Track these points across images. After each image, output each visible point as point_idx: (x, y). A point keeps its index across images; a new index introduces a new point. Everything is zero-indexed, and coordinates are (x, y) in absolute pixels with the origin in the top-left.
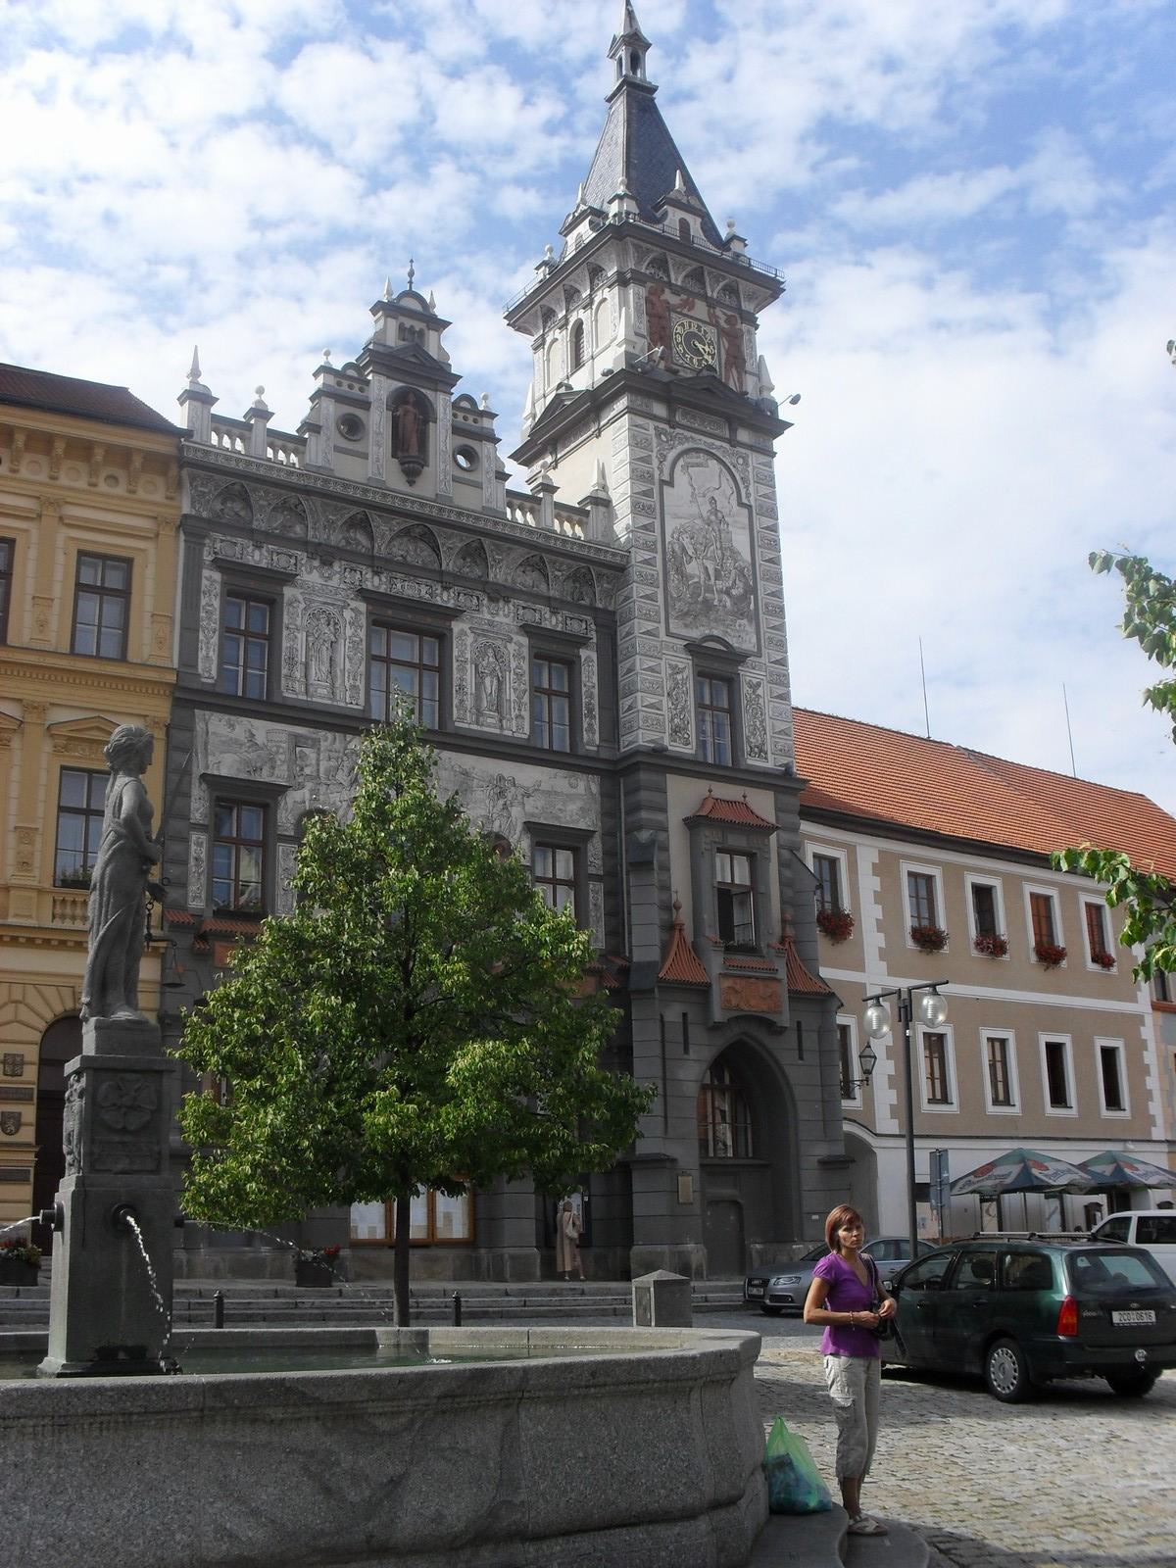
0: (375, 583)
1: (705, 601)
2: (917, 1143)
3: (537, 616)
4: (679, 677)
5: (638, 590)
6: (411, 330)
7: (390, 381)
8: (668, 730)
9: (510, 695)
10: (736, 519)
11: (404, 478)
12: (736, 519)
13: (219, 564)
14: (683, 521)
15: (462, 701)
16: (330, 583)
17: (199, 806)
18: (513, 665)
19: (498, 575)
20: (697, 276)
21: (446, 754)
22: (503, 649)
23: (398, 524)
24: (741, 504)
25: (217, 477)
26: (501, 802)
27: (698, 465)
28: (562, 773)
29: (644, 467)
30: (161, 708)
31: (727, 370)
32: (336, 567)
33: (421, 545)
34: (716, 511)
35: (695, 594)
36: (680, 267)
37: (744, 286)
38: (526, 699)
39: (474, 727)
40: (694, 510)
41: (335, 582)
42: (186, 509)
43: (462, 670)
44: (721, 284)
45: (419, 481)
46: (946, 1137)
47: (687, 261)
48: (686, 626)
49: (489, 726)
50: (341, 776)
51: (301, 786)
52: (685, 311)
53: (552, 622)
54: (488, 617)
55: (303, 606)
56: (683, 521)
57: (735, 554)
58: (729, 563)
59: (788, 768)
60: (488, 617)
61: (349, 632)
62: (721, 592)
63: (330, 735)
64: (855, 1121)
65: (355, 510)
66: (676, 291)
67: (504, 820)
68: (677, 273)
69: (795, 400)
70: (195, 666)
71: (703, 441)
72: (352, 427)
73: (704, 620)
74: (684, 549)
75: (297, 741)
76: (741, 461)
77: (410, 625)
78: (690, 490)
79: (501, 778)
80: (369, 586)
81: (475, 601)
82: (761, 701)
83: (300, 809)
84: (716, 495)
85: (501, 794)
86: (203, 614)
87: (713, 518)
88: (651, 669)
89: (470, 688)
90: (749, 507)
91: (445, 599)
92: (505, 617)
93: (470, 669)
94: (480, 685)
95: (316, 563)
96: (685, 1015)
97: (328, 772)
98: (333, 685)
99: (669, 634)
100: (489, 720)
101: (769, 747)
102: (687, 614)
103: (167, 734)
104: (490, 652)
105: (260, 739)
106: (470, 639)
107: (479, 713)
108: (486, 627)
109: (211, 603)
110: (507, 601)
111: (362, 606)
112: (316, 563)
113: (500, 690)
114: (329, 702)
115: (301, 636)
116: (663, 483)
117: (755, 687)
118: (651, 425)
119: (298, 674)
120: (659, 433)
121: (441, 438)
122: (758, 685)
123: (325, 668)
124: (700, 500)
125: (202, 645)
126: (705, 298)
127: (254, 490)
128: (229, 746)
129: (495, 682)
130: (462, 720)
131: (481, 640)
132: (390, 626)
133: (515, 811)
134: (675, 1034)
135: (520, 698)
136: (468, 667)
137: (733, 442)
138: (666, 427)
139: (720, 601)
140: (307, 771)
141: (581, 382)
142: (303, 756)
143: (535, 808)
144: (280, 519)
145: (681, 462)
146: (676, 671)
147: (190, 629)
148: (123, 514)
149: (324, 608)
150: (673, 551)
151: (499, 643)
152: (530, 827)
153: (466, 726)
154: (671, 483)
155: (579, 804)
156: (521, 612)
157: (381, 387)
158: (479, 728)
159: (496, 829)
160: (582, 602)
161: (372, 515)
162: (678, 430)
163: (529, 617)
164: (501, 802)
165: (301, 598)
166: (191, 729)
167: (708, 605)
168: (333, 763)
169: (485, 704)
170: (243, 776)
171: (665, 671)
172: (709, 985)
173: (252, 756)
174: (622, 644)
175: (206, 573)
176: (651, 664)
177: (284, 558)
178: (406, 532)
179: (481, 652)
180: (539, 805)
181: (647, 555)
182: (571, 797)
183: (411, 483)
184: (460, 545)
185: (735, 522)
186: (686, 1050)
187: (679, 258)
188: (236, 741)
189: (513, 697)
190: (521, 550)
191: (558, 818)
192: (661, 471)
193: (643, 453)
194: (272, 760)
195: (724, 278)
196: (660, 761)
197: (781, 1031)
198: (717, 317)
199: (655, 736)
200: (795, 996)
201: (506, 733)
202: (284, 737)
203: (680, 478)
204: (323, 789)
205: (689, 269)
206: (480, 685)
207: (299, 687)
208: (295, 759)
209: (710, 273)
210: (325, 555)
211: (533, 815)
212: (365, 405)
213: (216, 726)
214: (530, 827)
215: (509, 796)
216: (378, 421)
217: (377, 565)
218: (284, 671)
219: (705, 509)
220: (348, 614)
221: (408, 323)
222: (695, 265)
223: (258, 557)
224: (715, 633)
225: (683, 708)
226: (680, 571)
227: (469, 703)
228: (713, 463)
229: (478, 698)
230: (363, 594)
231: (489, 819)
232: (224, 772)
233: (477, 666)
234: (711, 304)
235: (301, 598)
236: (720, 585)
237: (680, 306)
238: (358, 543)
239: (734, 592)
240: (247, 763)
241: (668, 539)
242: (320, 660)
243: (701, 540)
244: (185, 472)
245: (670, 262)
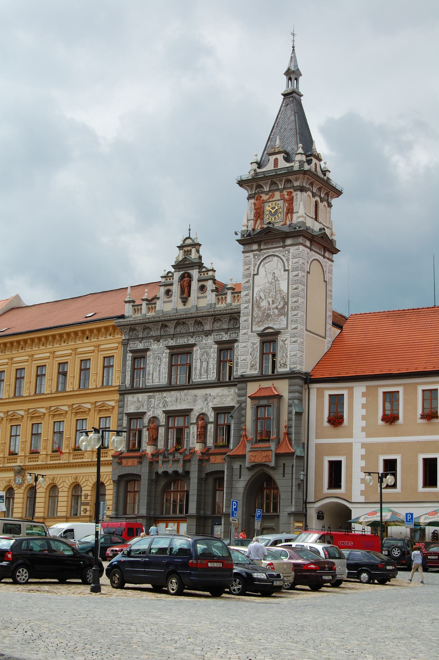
0: (172, 343)
1: (268, 314)
2: (384, 506)
3: (221, 336)
4: (255, 346)
5: (242, 319)
6: (188, 251)
7: (180, 272)
8: (249, 367)
9: (211, 366)
10: (283, 277)
11: (182, 304)
12: (283, 277)
13: (131, 351)
14: (261, 287)
15: (195, 373)
16: (160, 347)
18: (212, 356)
19: (207, 327)
20: (273, 183)
21: (190, 391)
22: (209, 351)
24: (285, 270)
26: (206, 402)
27: (269, 262)
28: (226, 388)
29: (248, 272)
30: (117, 397)
31: (286, 216)
32: (161, 341)
33: (185, 325)
36: (266, 184)
38: (216, 366)
39: (199, 380)
40: (266, 280)
41: (160, 346)
42: (124, 338)
43: (196, 362)
44: (283, 181)
45: (187, 304)
46: (431, 502)
47: (266, 181)
48: (259, 326)
49: (204, 379)
50: (161, 405)
51: (150, 410)
52: (271, 200)
53: (226, 337)
54: (205, 342)
55: (152, 356)
56: (261, 287)
57: (280, 291)
58: (278, 296)
60: (205, 342)
61: (164, 360)
62: (274, 308)
63: (158, 394)
64: (325, 498)
65: (161, 323)
66: (266, 193)
67: (206, 408)
68: (266, 187)
70: (125, 383)
71: (271, 252)
72: (168, 293)
73: (266, 321)
74: (261, 298)
75: (150, 397)
76: (287, 252)
78: (265, 273)
79: (206, 394)
80: (170, 344)
81: (201, 338)
82: (286, 346)
83: (150, 417)
85: (206, 400)
86: (127, 367)
87: (273, 281)
88: (245, 347)
89: (198, 368)
90: (288, 270)
91: (192, 341)
92: (210, 340)
93: (199, 361)
95: (156, 342)
96: (241, 466)
97: (157, 405)
98: (159, 378)
99: (252, 331)
100: (204, 376)
101: (288, 363)
102: (260, 322)
104: (205, 354)
105: (140, 400)
106: (199, 350)
107: (201, 374)
108: (204, 346)
110: (211, 335)
111: (168, 351)
112: (156, 342)
113: (207, 366)
114: (158, 383)
115: (151, 366)
116: (254, 275)
117: (284, 341)
118: (251, 254)
119: (150, 377)
120: (254, 255)
121: (195, 285)
122: (286, 340)
123: (157, 373)
124: (268, 276)
125: (127, 376)
126: (278, 190)
128: (133, 403)
129: (206, 363)
130: (195, 379)
131: (203, 350)
132: (178, 354)
134: (237, 472)
135: (214, 366)
136: (198, 361)
137: (284, 247)
138: (257, 252)
139: (273, 312)
140: (152, 406)
142: (151, 401)
143: (218, 403)
144: (147, 331)
145: (262, 263)
146: (254, 344)
147: (124, 372)
148: (111, 344)
149: (158, 355)
150: (257, 300)
151: (208, 350)
152: (214, 409)
153: (196, 380)
154: (257, 274)
155: (231, 397)
156: (215, 337)
157: (177, 275)
158: (200, 380)
159: (204, 412)
160: (237, 326)
161: (166, 323)
162: (262, 252)
163: (218, 338)
164: (206, 402)
165: (152, 354)
166: (124, 401)
167: (268, 316)
168: (159, 402)
169: (203, 371)
170: (135, 411)
171: (249, 345)
175: (128, 355)
176: (244, 345)
177: (147, 343)
178: (177, 324)
179: (202, 355)
180: (218, 400)
181: (246, 305)
182: (228, 396)
183: (184, 305)
184: (193, 322)
185: (282, 278)
186: (240, 478)
187: (263, 182)
188: (134, 402)
189: (212, 367)
190: (209, 318)
191: (224, 404)
192: (254, 270)
193: (247, 267)
194: (143, 405)
195: (283, 179)
196: (245, 380)
197: (273, 468)
198: (283, 195)
200: (278, 456)
201: (209, 379)
202: (146, 397)
203: (261, 269)
204: (156, 410)
205: (269, 183)
207: (150, 381)
208: (149, 403)
209: (277, 180)
210: (157, 339)
211: (216, 404)
213: (130, 398)
214: (214, 409)
215: (208, 400)
216: (176, 289)
217: (173, 336)
218: (147, 377)
219: (270, 277)
220: (164, 355)
221: (186, 249)
223: (140, 346)
224: (270, 325)
225: (256, 357)
226: (259, 307)
227: (198, 373)
228: (275, 259)
229: (201, 370)
230: (169, 347)
231: (202, 409)
232: (131, 411)
233: (201, 360)
234: (281, 191)
235: (152, 354)
236: (274, 306)
237: (269, 199)
238: (167, 331)
239: (279, 307)
240: (137, 407)
241: (255, 295)
242: (156, 371)
243: (268, 291)
245: (262, 184)
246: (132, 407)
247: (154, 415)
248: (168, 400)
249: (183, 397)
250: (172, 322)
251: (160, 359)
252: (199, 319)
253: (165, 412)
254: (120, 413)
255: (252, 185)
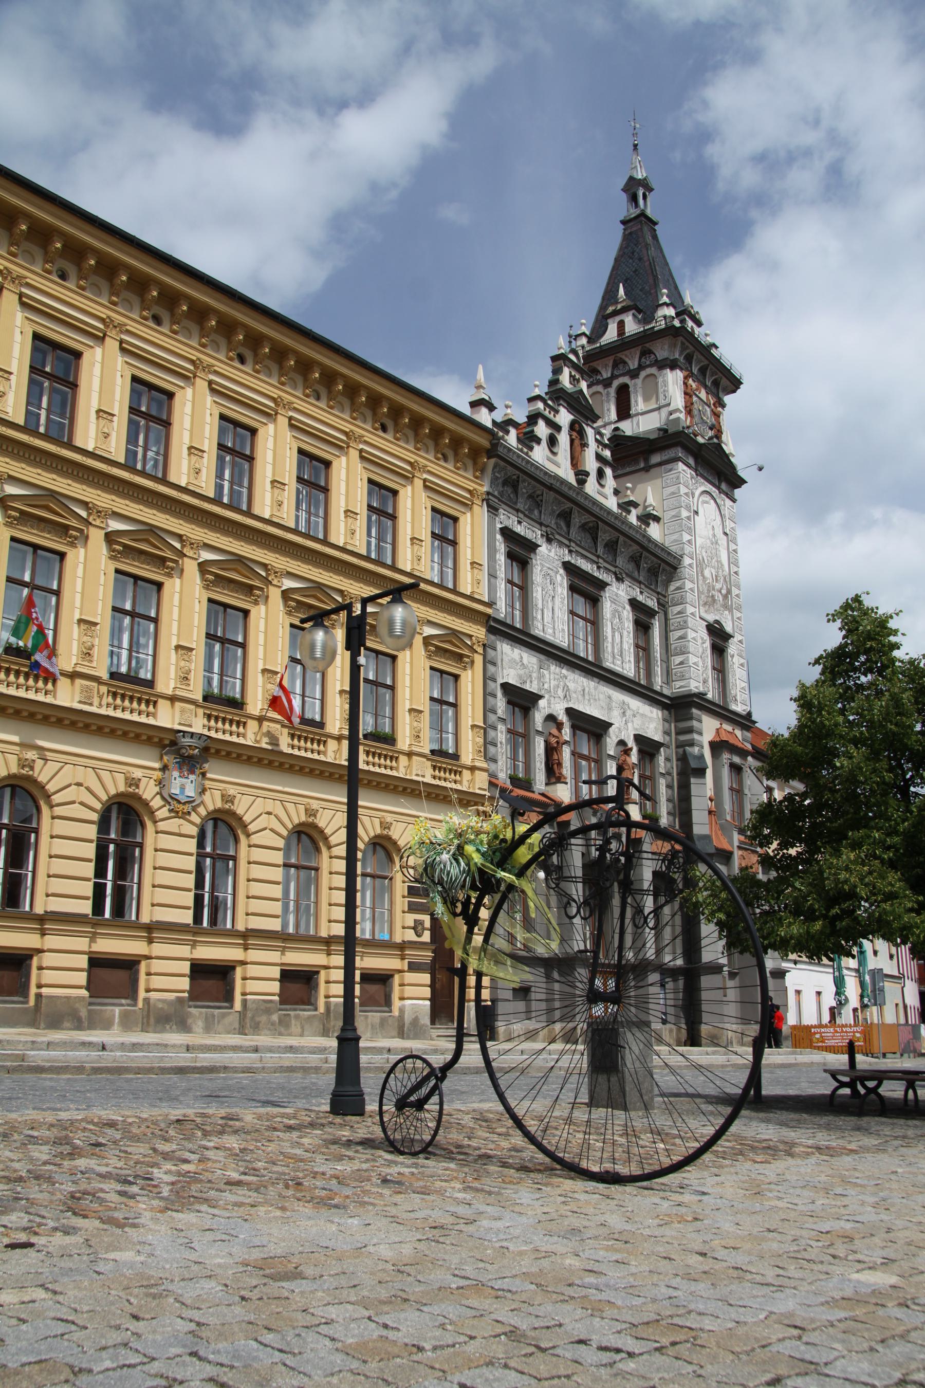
9: (625, 646)
17: (501, 704)
23: (586, 518)
25: (509, 468)
27: (707, 502)
33: (588, 535)
34: (714, 536)
35: (709, 591)
36: (699, 361)
37: (724, 382)
50: (560, 693)
59: (749, 714)
65: (569, 505)
69: (760, 469)
71: (709, 487)
77: (586, 590)
84: (714, 523)
89: (610, 639)
94: (613, 636)
103: (484, 650)
105: (525, 661)
107: (614, 657)
109: (501, 558)
115: (540, 589)
117: (732, 656)
127: (524, 481)
133: (630, 725)
140: (546, 686)
141: (628, 428)
142: (544, 676)
172: (731, 853)
173: (522, 672)
174: (674, 621)
199: (697, 684)
203: (701, 512)
206: (613, 636)
212: (558, 428)
219: (711, 532)
222: (706, 362)
226: (703, 575)
228: (712, 502)
236: (718, 586)
240: (520, 677)
244: (493, 461)
246: (512, 672)
247: (550, 712)
248: (572, 686)
249: (592, 691)
250: (587, 516)
251: (552, 583)
252: (622, 538)
253: (570, 712)
254: (488, 678)
255: (687, 348)
